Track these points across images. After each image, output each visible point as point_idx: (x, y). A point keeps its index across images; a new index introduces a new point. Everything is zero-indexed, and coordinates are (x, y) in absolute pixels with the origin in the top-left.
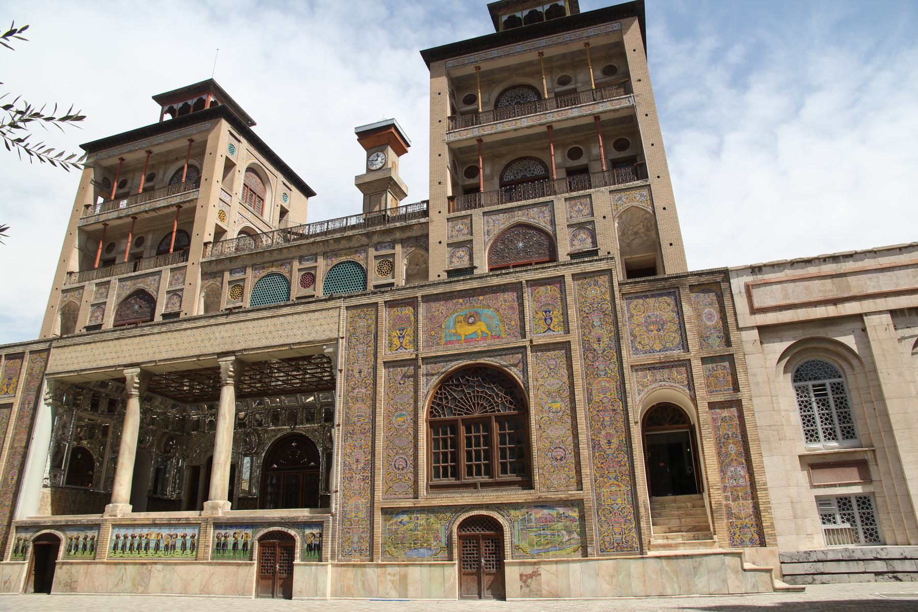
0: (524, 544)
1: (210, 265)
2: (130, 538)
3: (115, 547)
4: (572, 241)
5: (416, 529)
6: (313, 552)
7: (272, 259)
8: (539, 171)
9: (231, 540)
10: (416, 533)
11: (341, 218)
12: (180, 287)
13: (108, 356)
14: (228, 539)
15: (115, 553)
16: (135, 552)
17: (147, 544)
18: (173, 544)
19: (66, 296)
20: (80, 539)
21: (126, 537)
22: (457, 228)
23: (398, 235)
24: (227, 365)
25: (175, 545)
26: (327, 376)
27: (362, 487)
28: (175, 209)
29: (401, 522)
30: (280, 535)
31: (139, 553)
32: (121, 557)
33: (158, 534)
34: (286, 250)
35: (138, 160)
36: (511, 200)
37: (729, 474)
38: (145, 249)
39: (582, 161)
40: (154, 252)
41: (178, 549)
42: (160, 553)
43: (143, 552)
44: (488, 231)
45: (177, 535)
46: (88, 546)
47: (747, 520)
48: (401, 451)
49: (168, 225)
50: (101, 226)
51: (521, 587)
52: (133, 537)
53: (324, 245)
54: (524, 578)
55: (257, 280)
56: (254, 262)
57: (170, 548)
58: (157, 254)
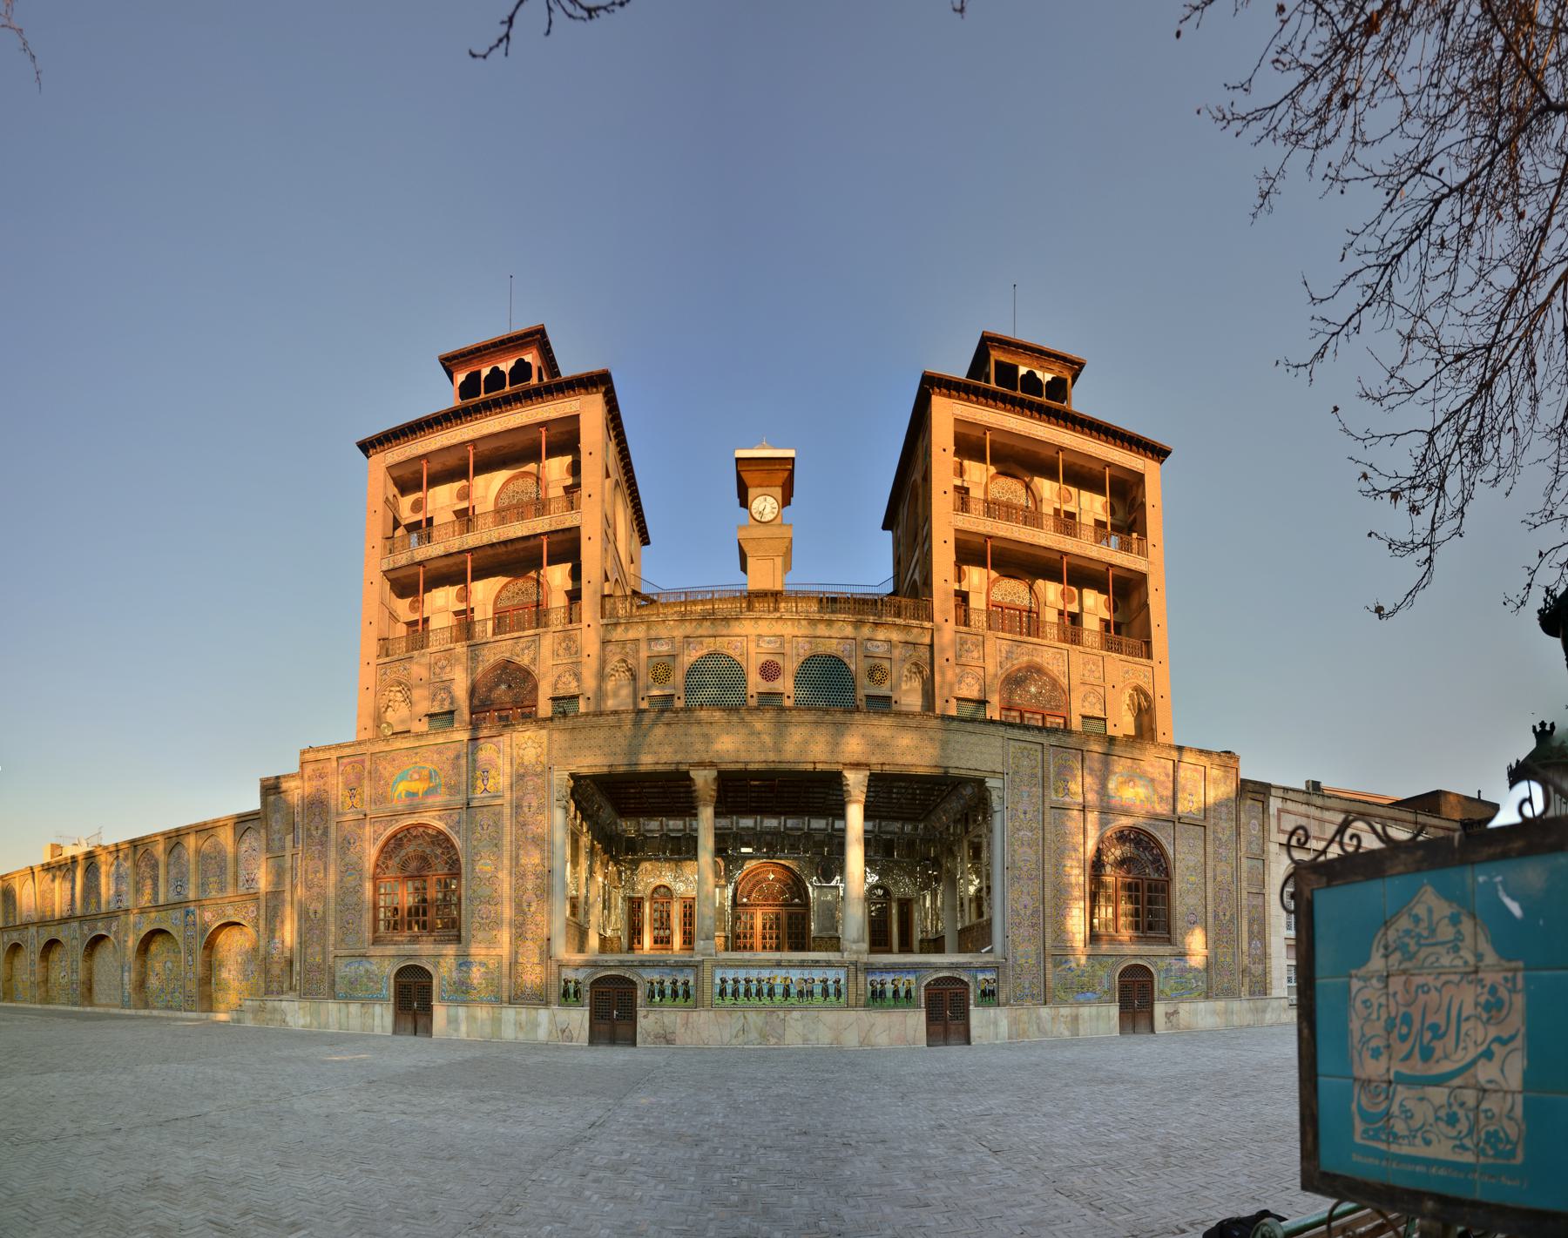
42: (793, 1000)
43: (766, 1000)
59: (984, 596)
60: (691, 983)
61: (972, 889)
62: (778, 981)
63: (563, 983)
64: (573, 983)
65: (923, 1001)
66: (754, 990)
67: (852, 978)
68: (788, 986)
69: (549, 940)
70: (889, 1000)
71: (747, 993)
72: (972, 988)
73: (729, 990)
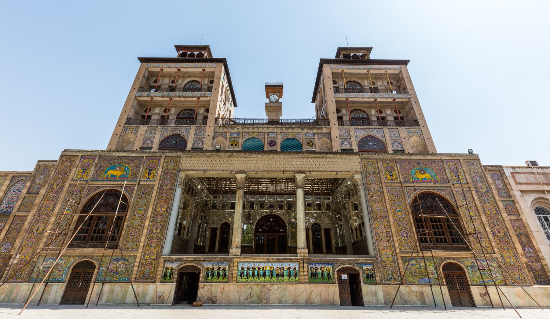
0: (476, 278)
1: (219, 128)
2: (251, 269)
3: (242, 275)
4: (393, 145)
5: (420, 268)
6: (370, 279)
7: (254, 131)
8: (365, 116)
9: (319, 271)
10: (421, 270)
11: (260, 119)
12: (202, 136)
13: (223, 165)
14: (318, 271)
15: (242, 278)
18: (282, 273)
19: (126, 130)
20: (215, 270)
21: (248, 269)
22: (343, 132)
23: (316, 131)
24: (300, 178)
25: (283, 274)
27: (387, 245)
29: (412, 264)
30: (344, 269)
31: (259, 279)
32: (247, 281)
33: (271, 267)
36: (364, 125)
37: (526, 251)
38: (171, 114)
39: (383, 115)
40: (175, 117)
41: (286, 277)
42: (274, 279)
43: (262, 279)
44: (357, 136)
45: (284, 268)
47: (540, 272)
48: (404, 229)
50: (149, 99)
51: (482, 300)
52: (254, 269)
53: (280, 129)
54: (482, 295)
55: (245, 139)
56: (244, 131)
58: (177, 118)
59: (348, 116)
60: (227, 269)
61: (356, 224)
62: (268, 269)
63: (165, 270)
64: (170, 270)
65: (336, 279)
66: (256, 274)
67: (301, 267)
68: (272, 271)
69: (162, 247)
70: (319, 278)
71: (253, 274)
72: (361, 274)
73: (245, 274)
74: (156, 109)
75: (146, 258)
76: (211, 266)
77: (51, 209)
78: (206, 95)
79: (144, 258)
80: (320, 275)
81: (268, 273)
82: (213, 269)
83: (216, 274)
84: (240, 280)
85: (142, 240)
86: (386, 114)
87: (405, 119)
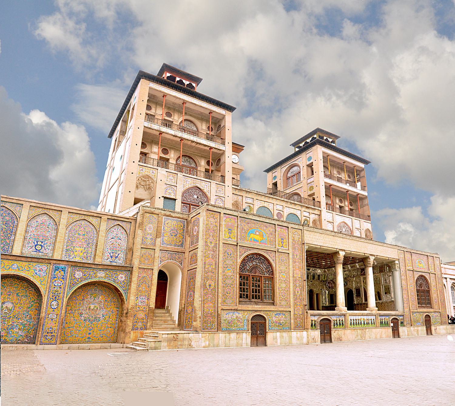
3: (351, 324)
9: (383, 320)
16: (360, 325)
17: (361, 322)
19: (142, 170)
23: (311, 211)
26: (323, 263)
28: (208, 148)
34: (271, 199)
35: (175, 104)
39: (342, 205)
41: (370, 324)
42: (365, 326)
46: (341, 324)
49: (185, 151)
52: (356, 320)
53: (286, 203)
57: (368, 324)
60: (343, 320)
64: (314, 321)
74: (154, 146)
75: (296, 313)
76: (335, 319)
77: (214, 267)
78: (221, 148)
79: (295, 313)
80: (384, 323)
81: (363, 323)
82: (337, 321)
83: (338, 323)
84: (350, 327)
85: (292, 300)
86: (345, 205)
87: (354, 211)
